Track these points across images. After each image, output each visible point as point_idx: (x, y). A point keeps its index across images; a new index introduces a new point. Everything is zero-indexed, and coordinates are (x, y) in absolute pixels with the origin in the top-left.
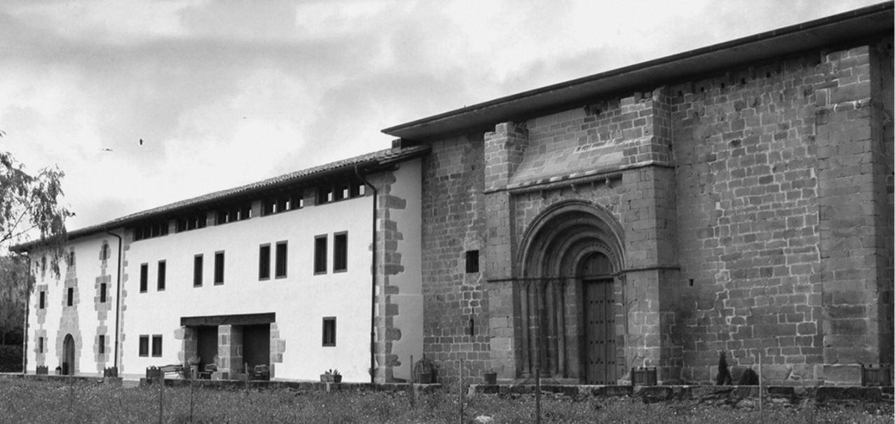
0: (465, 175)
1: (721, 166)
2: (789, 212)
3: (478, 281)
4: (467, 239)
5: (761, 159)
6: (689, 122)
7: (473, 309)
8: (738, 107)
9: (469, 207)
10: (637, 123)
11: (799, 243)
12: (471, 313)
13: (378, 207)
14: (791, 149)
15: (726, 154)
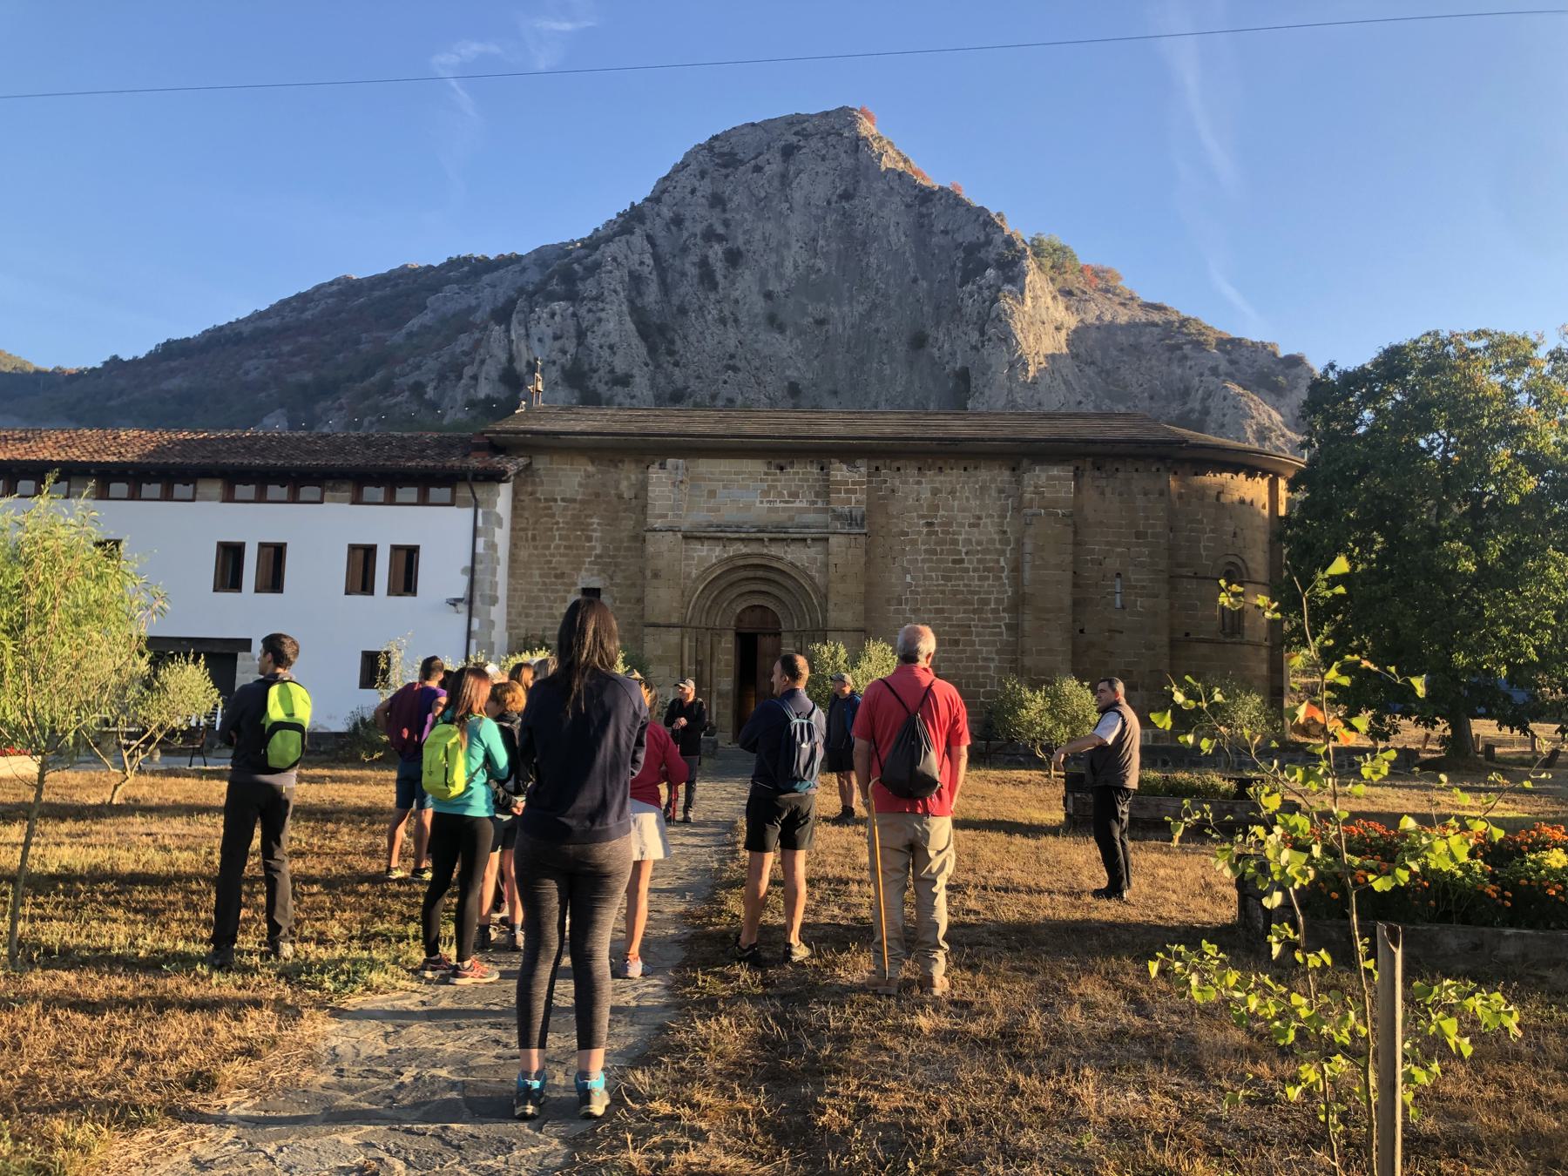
0: (582, 502)
1: (913, 542)
2: (979, 593)
4: (583, 573)
5: (955, 542)
6: (883, 497)
8: (935, 492)
9: (589, 539)
10: (847, 491)
11: (986, 620)
13: (480, 523)
14: (984, 538)
15: (919, 533)
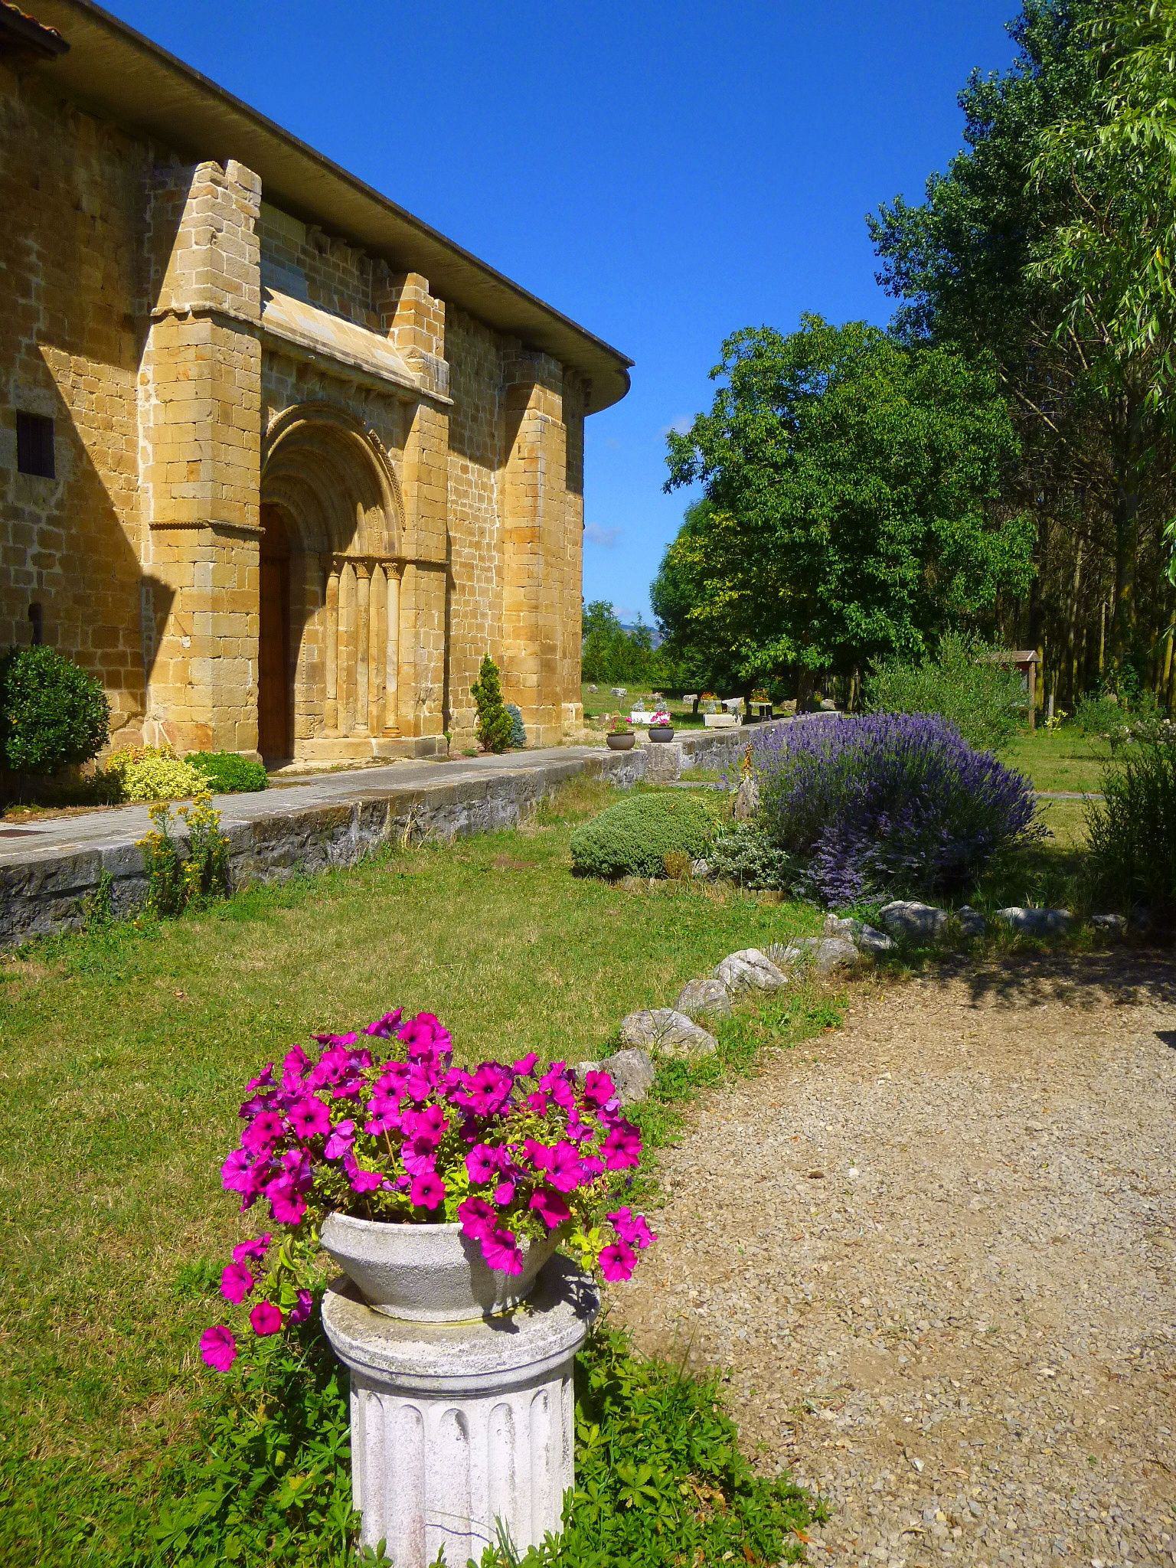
3: (53, 501)
7: (40, 575)
12: (35, 585)
